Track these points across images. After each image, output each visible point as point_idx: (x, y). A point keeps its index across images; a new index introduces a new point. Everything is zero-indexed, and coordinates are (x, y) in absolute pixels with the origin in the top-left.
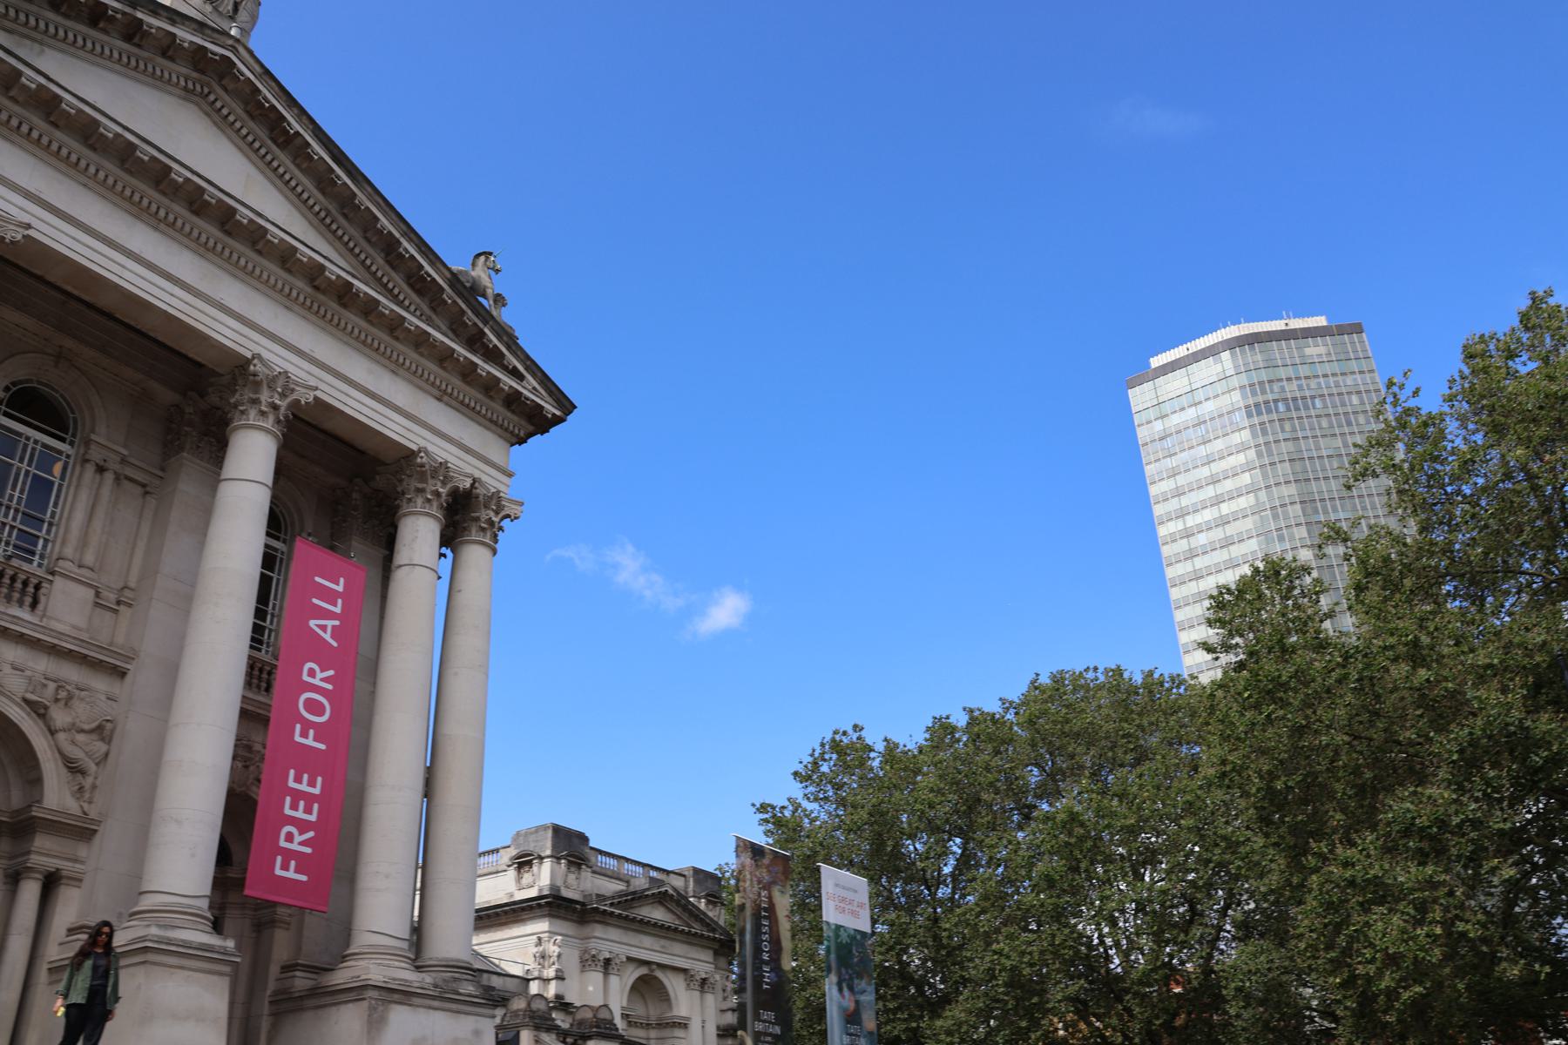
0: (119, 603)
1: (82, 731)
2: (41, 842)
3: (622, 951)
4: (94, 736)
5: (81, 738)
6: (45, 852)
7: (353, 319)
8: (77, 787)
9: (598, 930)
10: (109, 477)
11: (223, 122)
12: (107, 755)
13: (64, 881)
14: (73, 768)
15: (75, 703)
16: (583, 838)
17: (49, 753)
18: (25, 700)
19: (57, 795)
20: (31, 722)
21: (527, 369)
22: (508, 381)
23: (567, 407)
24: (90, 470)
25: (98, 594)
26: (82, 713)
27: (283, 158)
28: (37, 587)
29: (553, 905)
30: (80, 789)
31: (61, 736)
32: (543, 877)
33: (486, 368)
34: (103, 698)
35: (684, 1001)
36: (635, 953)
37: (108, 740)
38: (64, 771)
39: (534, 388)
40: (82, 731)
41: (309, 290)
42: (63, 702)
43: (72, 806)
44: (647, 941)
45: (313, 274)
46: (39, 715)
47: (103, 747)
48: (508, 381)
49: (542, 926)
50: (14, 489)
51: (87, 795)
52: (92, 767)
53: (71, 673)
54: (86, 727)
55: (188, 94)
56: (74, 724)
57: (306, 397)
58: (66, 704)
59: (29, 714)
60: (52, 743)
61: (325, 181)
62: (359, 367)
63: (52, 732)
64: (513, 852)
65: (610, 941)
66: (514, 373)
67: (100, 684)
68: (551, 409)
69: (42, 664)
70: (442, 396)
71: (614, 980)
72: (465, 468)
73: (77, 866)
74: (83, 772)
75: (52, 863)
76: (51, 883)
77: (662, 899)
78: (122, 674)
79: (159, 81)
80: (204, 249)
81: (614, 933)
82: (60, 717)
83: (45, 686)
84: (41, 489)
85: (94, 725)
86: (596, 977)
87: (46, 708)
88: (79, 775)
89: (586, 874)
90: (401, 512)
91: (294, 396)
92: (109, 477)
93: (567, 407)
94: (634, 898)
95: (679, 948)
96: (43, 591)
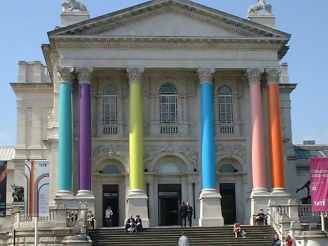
1: (192, 155)
2: (190, 178)
7: (220, 44)
10: (184, 99)
11: (177, 13)
18: (181, 153)
21: (273, 32)
23: (289, 36)
24: (180, 99)
27: (193, 13)
33: (259, 38)
39: (277, 36)
40: (192, 155)
41: (207, 44)
45: (206, 41)
47: (197, 157)
52: (195, 162)
53: (188, 143)
55: (167, 11)
57: (213, 71)
62: (228, 54)
66: (271, 35)
67: (194, 144)
68: (283, 39)
69: (181, 144)
70: (253, 49)
72: (260, 66)
74: (193, 163)
76: (194, 185)
79: (159, 13)
80: (181, 48)
82: (187, 153)
90: (250, 83)
91: (211, 72)
92: (184, 99)
93: (289, 36)
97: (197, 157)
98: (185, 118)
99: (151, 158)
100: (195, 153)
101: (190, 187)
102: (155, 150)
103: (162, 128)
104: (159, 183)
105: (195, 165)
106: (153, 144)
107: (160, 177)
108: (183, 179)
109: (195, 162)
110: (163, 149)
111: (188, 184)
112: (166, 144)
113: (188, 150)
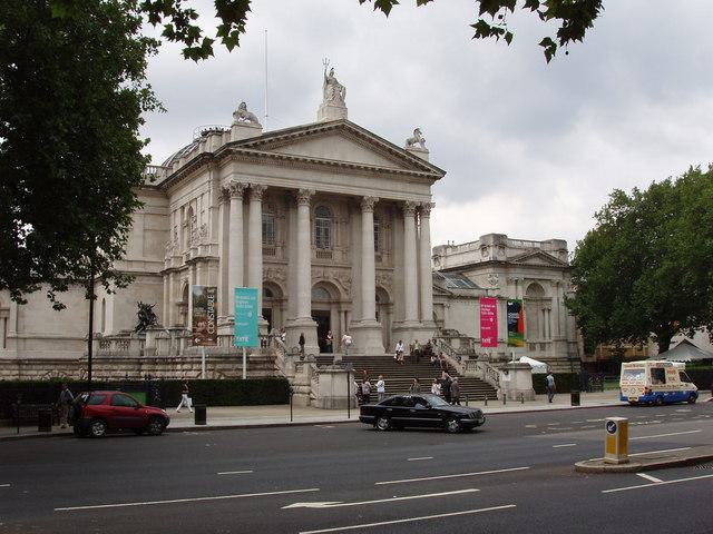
3: (522, 277)
6: (344, 307)
9: (512, 271)
16: (504, 236)
19: (344, 296)
22: (427, 174)
29: (495, 263)
32: (491, 254)
35: (550, 292)
36: (528, 276)
44: (532, 271)
48: (427, 174)
49: (491, 270)
53: (342, 270)
61: (370, 140)
64: (477, 246)
65: (517, 274)
71: (520, 288)
76: (346, 312)
77: (539, 255)
81: (518, 270)
84: (327, 230)
86: (513, 287)
89: (508, 250)
94: (525, 258)
95: (546, 272)
101: (343, 315)
111: (340, 312)
112: (322, 270)
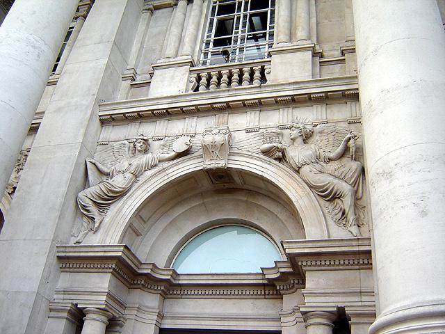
0: (343, 54)
1: (330, 160)
2: (313, 280)
4: (345, 160)
5: (333, 166)
8: (340, 214)
12: (363, 170)
13: (353, 320)
14: (332, 197)
15: (316, 138)
17: (300, 190)
20: (273, 169)
25: (315, 54)
26: (323, 145)
28: (263, 70)
30: (343, 214)
31: (302, 170)
34: (345, 125)
37: (359, 154)
38: (322, 201)
40: (330, 160)
42: (300, 140)
43: (339, 232)
46: (279, 159)
47: (355, 166)
50: (237, 28)
51: (351, 217)
52: (345, 188)
53: (307, 116)
54: (332, 155)
56: (318, 158)
58: (305, 142)
59: (269, 163)
60: (300, 180)
63: (298, 172)
67: (339, 113)
73: (364, 298)
75: (331, 303)
78: (355, 97)
82: (297, 153)
83: (282, 135)
85: (339, 149)
87: (283, 153)
88: (337, 200)
96: (266, 72)
97: (355, 166)
98: (301, 33)
99: (119, 182)
100: (347, 149)
102: (146, 151)
103: (199, 78)
104: (168, 324)
105: (347, 203)
106: (150, 130)
107: (172, 288)
108: (289, 302)
109: (345, 188)
110: (180, 146)
113: (307, 137)
